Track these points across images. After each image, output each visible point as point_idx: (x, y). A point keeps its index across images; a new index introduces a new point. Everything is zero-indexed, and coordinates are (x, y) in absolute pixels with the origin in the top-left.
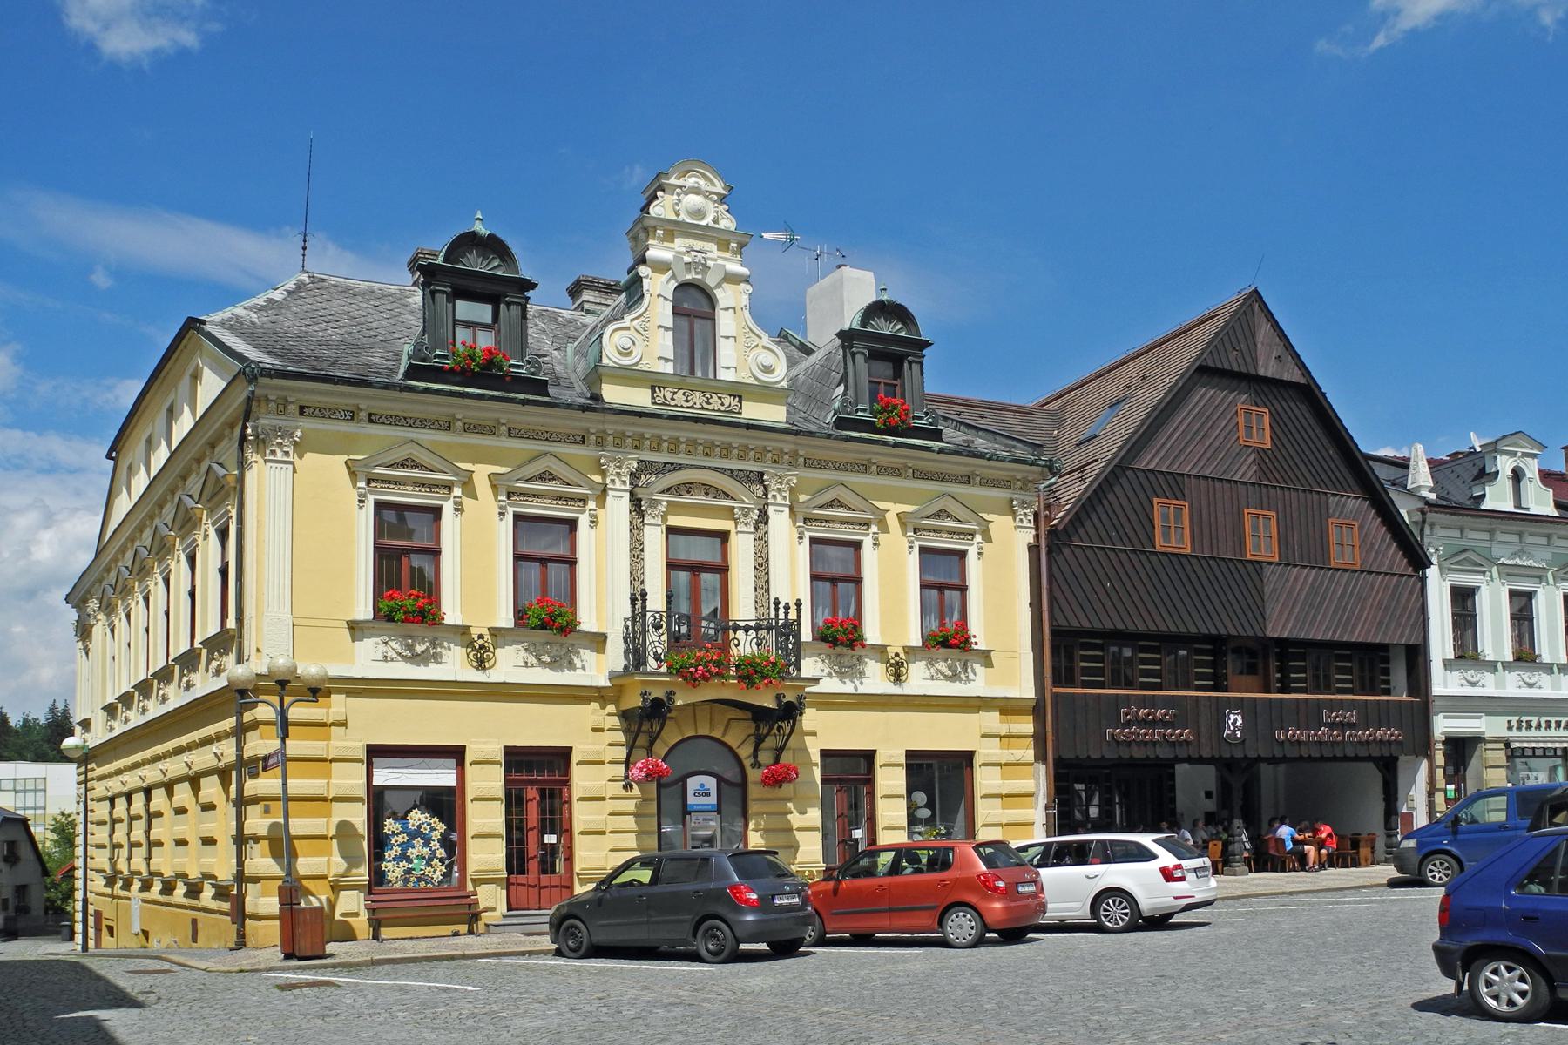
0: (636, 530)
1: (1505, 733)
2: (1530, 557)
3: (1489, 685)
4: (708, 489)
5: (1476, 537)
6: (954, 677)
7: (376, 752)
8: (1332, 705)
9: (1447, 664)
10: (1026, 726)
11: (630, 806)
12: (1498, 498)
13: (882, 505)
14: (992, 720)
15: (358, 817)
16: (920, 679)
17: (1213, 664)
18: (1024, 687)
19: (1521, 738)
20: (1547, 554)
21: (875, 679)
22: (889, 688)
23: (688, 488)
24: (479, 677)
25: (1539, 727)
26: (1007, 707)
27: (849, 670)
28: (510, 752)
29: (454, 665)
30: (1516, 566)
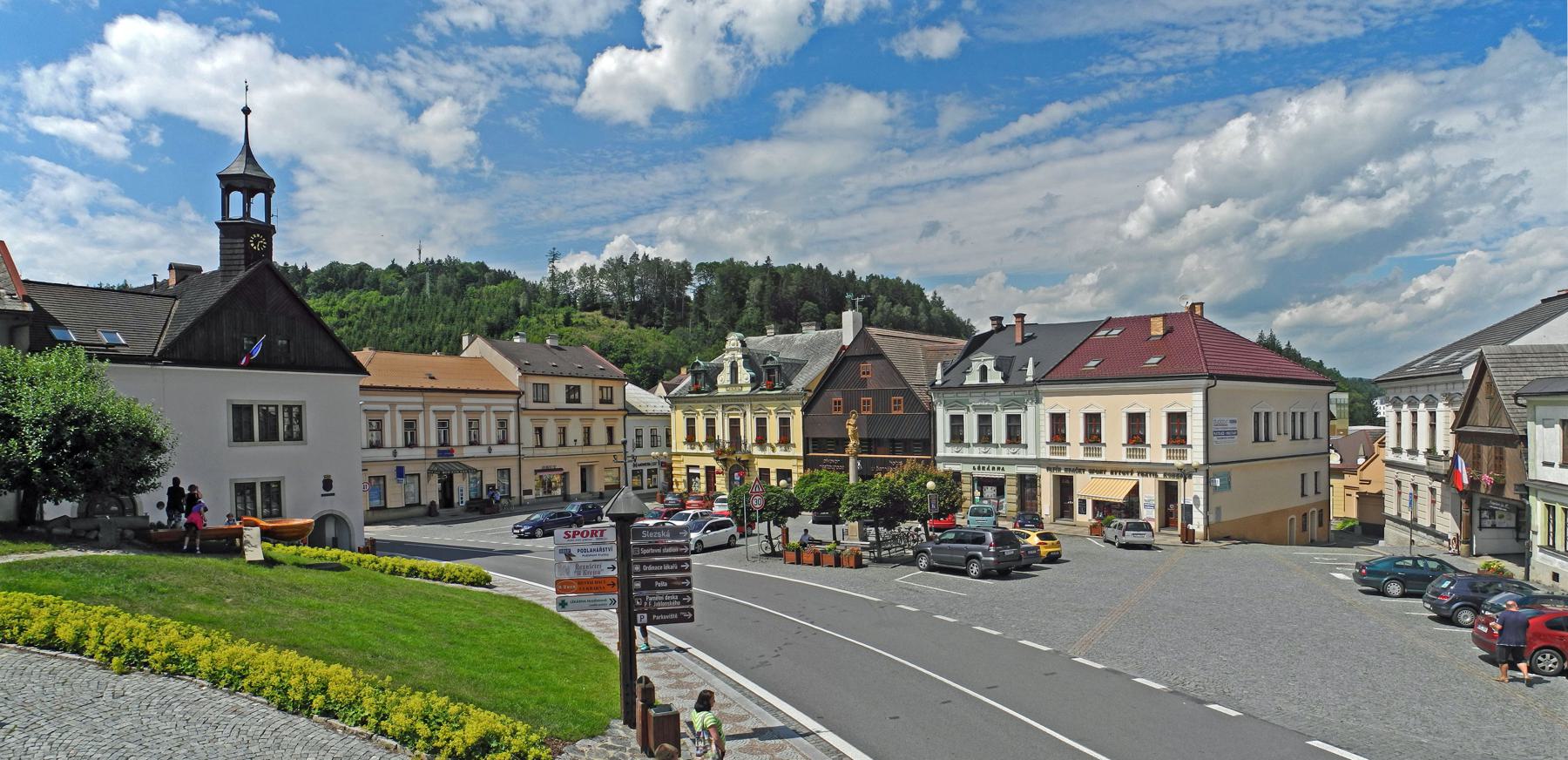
2: (988, 401)
3: (965, 453)
5: (962, 396)
6: (786, 450)
7: (688, 467)
8: (894, 459)
9: (947, 445)
10: (801, 463)
12: (973, 379)
13: (769, 408)
14: (795, 462)
15: (685, 478)
16: (779, 451)
17: (868, 448)
18: (801, 454)
19: (978, 474)
20: (998, 399)
21: (769, 452)
22: (772, 454)
23: (732, 410)
25: (988, 469)
26: (797, 458)
27: (763, 449)
29: (697, 450)
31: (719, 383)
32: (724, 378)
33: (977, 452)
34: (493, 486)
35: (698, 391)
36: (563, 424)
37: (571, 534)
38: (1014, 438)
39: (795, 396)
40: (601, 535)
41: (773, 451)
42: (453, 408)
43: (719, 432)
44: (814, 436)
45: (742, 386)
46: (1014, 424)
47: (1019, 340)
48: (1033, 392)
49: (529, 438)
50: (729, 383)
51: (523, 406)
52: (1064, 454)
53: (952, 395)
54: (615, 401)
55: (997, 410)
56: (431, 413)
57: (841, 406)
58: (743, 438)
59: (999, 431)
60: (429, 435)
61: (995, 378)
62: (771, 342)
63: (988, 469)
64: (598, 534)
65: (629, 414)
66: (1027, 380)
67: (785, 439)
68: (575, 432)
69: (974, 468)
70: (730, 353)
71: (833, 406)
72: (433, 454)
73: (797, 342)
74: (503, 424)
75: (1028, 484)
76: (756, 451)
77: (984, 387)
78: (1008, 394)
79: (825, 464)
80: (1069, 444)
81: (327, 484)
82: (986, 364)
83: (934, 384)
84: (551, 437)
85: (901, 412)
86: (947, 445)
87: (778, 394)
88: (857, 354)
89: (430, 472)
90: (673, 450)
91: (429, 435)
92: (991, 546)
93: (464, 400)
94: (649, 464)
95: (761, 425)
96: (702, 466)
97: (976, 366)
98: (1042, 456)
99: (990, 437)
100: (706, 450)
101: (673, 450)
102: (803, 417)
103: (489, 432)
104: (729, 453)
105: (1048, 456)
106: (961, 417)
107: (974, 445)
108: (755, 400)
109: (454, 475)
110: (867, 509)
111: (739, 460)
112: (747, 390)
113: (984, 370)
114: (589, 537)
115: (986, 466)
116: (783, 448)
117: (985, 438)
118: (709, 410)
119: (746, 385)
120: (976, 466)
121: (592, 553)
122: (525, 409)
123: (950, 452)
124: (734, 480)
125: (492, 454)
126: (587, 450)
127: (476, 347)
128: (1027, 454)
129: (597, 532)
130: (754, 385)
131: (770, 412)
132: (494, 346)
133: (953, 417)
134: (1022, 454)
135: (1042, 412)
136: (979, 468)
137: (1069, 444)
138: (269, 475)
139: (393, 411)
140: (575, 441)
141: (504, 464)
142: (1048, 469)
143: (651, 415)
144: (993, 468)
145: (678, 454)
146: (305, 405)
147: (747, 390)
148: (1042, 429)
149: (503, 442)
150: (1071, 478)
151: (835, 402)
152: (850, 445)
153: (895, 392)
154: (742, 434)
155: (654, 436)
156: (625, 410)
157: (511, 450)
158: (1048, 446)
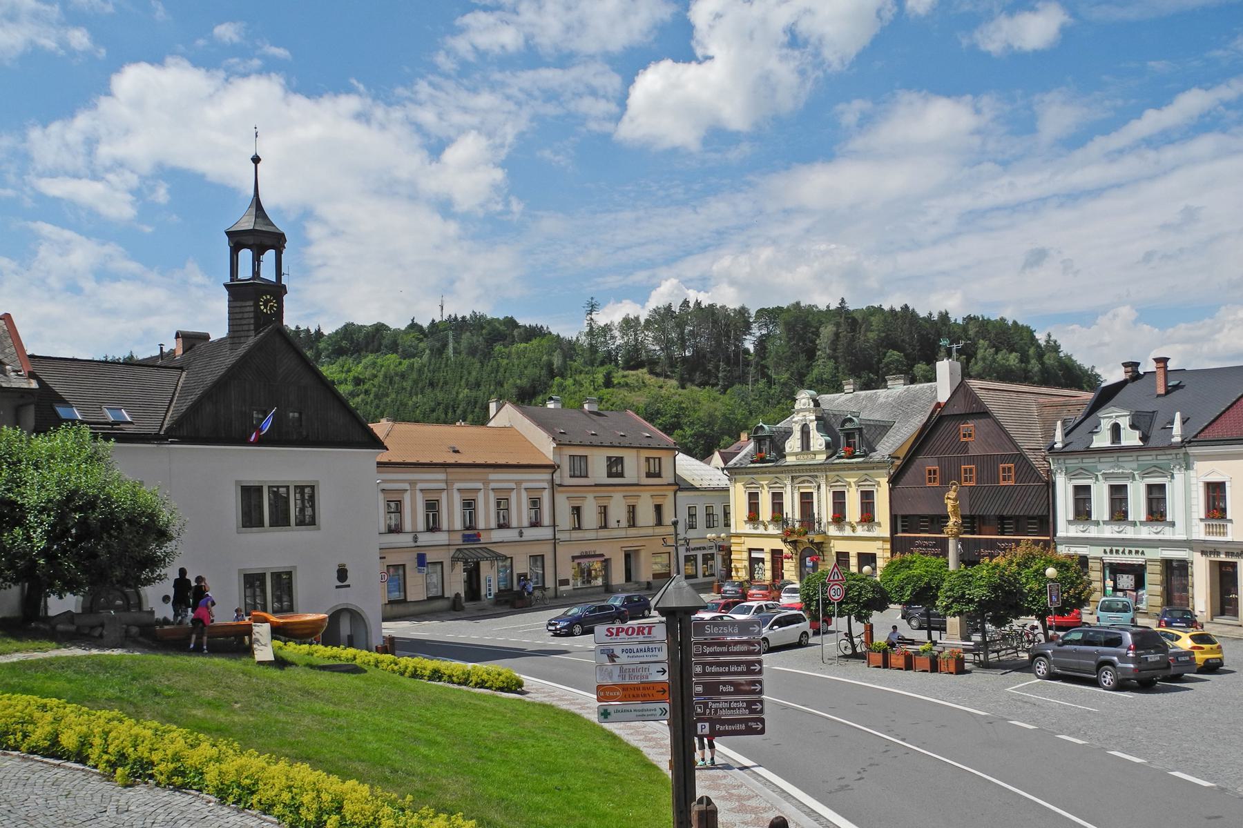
0: (792, 493)
1: (1101, 554)
2: (1123, 468)
3: (1093, 532)
4: (808, 481)
5: (1089, 462)
6: (869, 530)
7: (750, 550)
9: (1069, 522)
10: (888, 546)
11: (793, 564)
12: (1102, 440)
13: (848, 480)
14: (880, 544)
15: (747, 563)
16: (861, 531)
18: (887, 534)
21: (848, 532)
23: (803, 482)
24: (766, 532)
26: (883, 539)
27: (841, 529)
28: (772, 550)
29: (761, 530)
30: (1113, 473)
31: (788, 450)
32: (793, 444)
33: (1109, 532)
34: (525, 575)
35: (763, 460)
36: (603, 502)
37: (614, 631)
38: (1156, 512)
39: (879, 465)
40: (649, 633)
41: (853, 531)
42: (480, 485)
43: (787, 508)
44: (903, 513)
45: (815, 453)
46: (1156, 496)
47: (1161, 390)
48: (1182, 456)
49: (565, 519)
50: (800, 450)
51: (557, 481)
52: (1224, 534)
53: (1076, 461)
54: (663, 474)
55: (1134, 478)
56: (455, 491)
57: (937, 476)
58: (816, 516)
59: (1137, 504)
60: (452, 516)
61: (1131, 438)
62: (850, 400)
63: (1123, 552)
64: (646, 631)
65: (681, 489)
66: (1173, 440)
67: (868, 516)
68: (618, 512)
69: (1105, 552)
70: (801, 414)
71: (927, 476)
72: (458, 539)
73: (881, 400)
74: (535, 503)
75: (1176, 572)
76: (833, 531)
77: (1116, 451)
78: (1148, 459)
79: (917, 547)
80: (1231, 521)
81: (342, 574)
82: (1119, 421)
83: (1052, 447)
84: (590, 517)
85: (1011, 483)
86: (1069, 522)
87: (860, 463)
88: (956, 413)
89: (454, 560)
90: (733, 531)
91: (452, 516)
92: (1129, 649)
93: (492, 476)
94: (704, 548)
95: (839, 500)
96: (767, 549)
97: (1106, 425)
98: (1195, 537)
99: (1126, 513)
100: (772, 530)
101: (733, 531)
102: (891, 490)
103: (520, 512)
104: (800, 534)
105: (1202, 536)
106: (1088, 488)
107: (1105, 522)
108: (831, 470)
109: (481, 562)
110: (971, 601)
111: (812, 542)
112: (821, 458)
113: (1116, 429)
114: (635, 635)
115: (1121, 549)
116: (866, 527)
117: (1119, 513)
118: (776, 483)
119: (820, 452)
120: (1108, 549)
121: (638, 654)
122: (560, 485)
123: (1074, 531)
124: (806, 566)
125: (523, 539)
126: (632, 532)
127: (505, 416)
128: (1174, 534)
129: (644, 628)
130: (830, 452)
131: (850, 484)
132: (524, 413)
133: (1078, 489)
134: (1167, 534)
135: (1194, 481)
136: (1111, 551)
137: (1231, 521)
138: (279, 564)
139: (413, 490)
140: (618, 522)
141: (536, 550)
142: (1203, 553)
143: (706, 490)
144: (1130, 552)
145: (738, 536)
146: (318, 486)
147: (821, 458)
148: (1194, 502)
149: (536, 524)
150: (1234, 565)
151: (930, 471)
152: (950, 523)
153: (1004, 459)
154: (816, 511)
155: (710, 515)
156: (676, 484)
157: (544, 533)
158: (1202, 524)
